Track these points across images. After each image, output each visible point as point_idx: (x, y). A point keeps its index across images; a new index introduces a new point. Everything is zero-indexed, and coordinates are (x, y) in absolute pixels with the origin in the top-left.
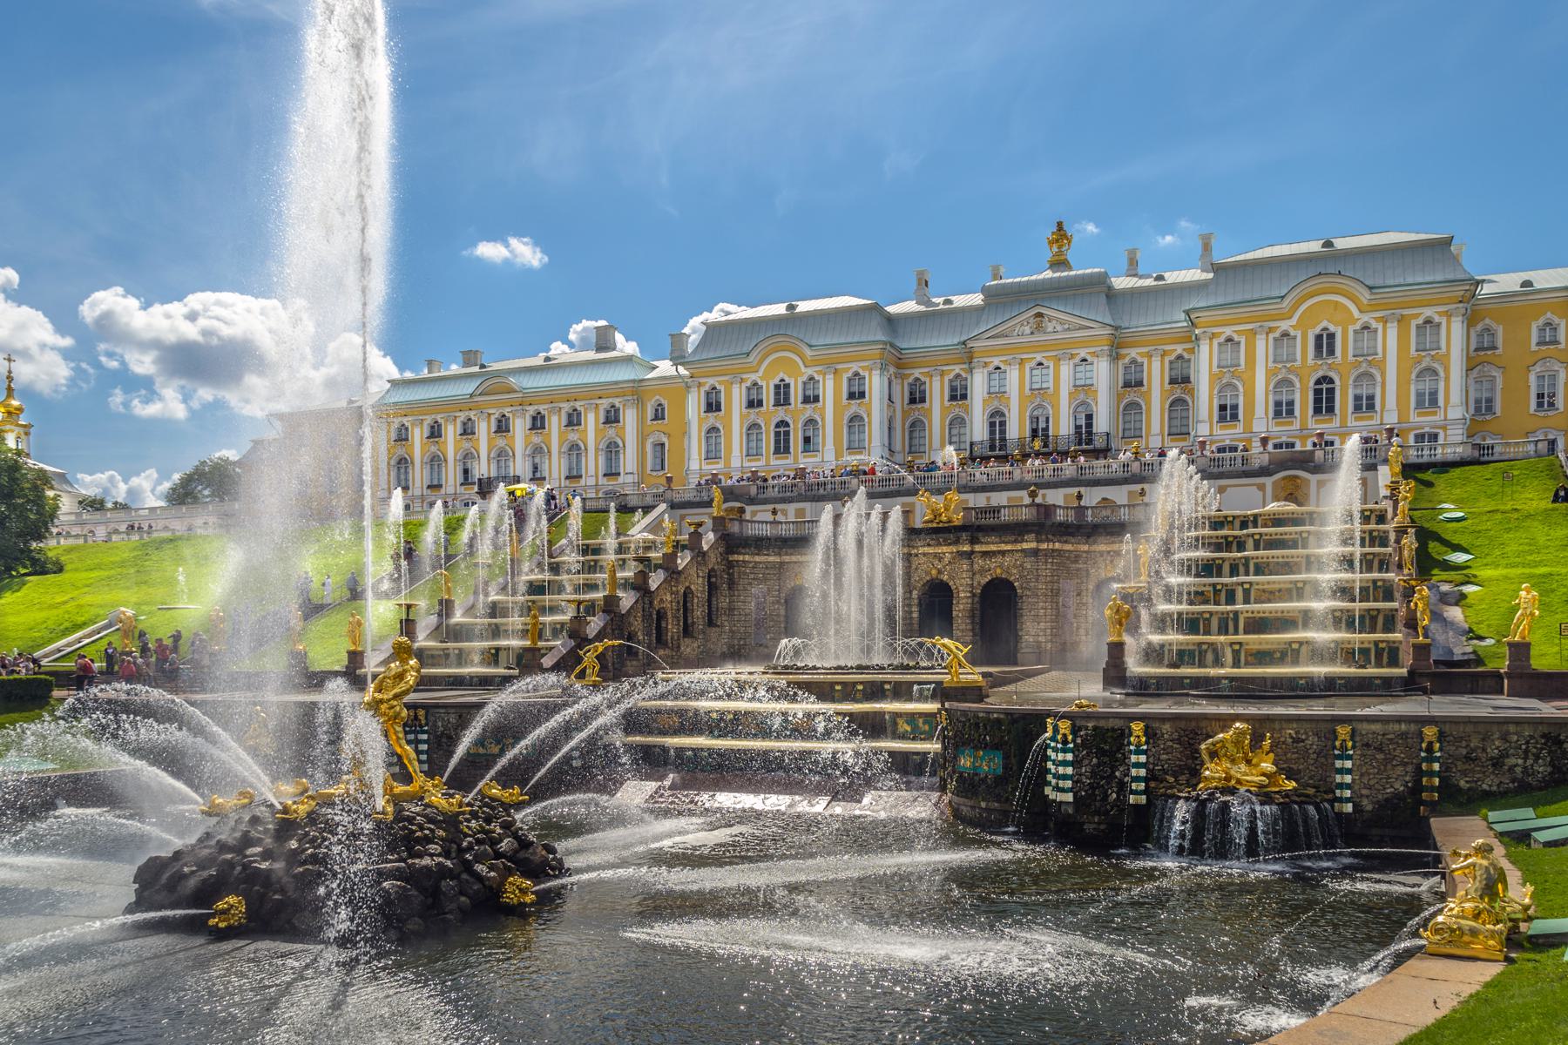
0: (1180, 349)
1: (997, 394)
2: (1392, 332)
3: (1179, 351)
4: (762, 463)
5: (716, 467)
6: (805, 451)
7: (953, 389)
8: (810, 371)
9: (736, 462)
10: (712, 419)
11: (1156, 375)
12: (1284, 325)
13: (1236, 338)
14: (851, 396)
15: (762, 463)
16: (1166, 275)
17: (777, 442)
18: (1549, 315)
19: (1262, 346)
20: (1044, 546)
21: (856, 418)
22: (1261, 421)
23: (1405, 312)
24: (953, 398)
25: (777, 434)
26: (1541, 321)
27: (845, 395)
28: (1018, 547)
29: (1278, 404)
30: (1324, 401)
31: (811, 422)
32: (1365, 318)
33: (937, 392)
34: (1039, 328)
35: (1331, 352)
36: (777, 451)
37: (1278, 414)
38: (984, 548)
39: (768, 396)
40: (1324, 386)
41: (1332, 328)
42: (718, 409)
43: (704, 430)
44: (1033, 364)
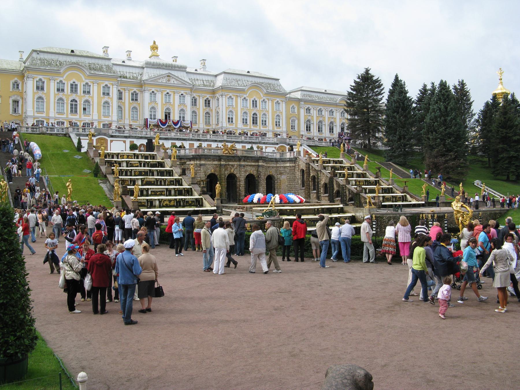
0: (208, 96)
1: (153, 101)
2: (270, 103)
4: (64, 116)
5: (41, 116)
6: (84, 113)
8: (87, 81)
9: (52, 114)
10: (40, 94)
11: (201, 102)
14: (104, 94)
15: (64, 116)
16: (198, 70)
17: (72, 108)
18: (293, 104)
19: (240, 100)
21: (106, 103)
22: (240, 125)
24: (132, 100)
25: (72, 105)
26: (291, 106)
28: (257, 164)
29: (243, 119)
30: (255, 122)
31: (87, 101)
32: (264, 98)
34: (169, 80)
35: (256, 106)
36: (72, 111)
38: (247, 163)
39: (67, 89)
40: (255, 116)
42: (42, 89)
43: (36, 98)
44: (166, 92)
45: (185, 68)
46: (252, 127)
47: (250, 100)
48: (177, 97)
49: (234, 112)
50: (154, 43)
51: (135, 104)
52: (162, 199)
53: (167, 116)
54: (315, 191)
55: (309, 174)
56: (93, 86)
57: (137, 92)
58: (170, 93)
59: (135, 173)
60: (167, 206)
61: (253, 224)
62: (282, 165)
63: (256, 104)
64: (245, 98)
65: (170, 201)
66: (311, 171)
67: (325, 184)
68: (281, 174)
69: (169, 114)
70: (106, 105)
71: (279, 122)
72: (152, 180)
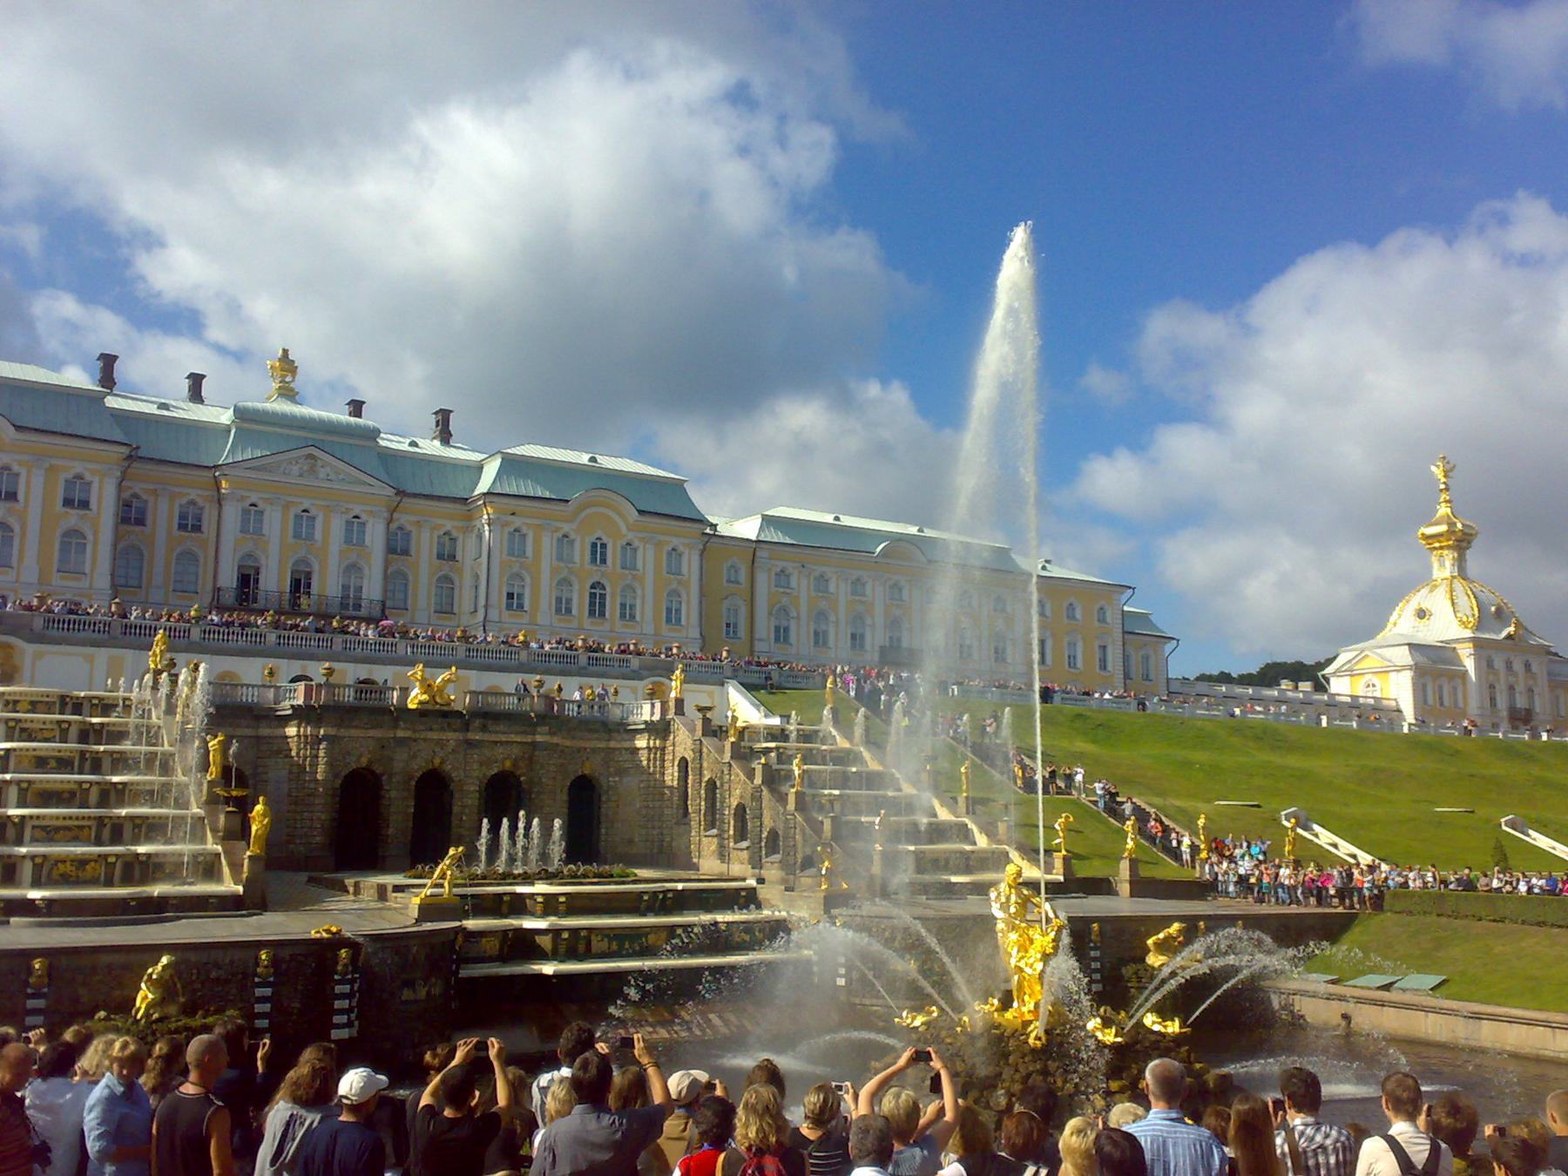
0: (449, 525)
3: (448, 527)
7: (183, 517)
12: (566, 528)
13: (524, 530)
14: (68, 502)
19: (548, 544)
20: (555, 740)
22: (545, 614)
23: (662, 538)
27: (59, 501)
29: (559, 600)
33: (163, 516)
34: (312, 470)
35: (604, 561)
37: (558, 611)
38: (494, 738)
40: (598, 591)
41: (605, 540)
45: (373, 434)
46: (587, 622)
47: (583, 542)
48: (337, 526)
49: (528, 580)
50: (285, 352)
51: (190, 540)
52: (45, 857)
53: (300, 584)
54: (715, 831)
55: (701, 774)
56: (28, 476)
57: (200, 502)
58: (313, 512)
59: (19, 762)
60: (66, 881)
61: (286, 953)
62: (627, 744)
63: (603, 554)
64: (565, 536)
65: (82, 862)
66: (705, 765)
67: (741, 811)
68: (621, 772)
69: (309, 575)
70: (74, 541)
71: (678, 611)
72: (66, 786)
